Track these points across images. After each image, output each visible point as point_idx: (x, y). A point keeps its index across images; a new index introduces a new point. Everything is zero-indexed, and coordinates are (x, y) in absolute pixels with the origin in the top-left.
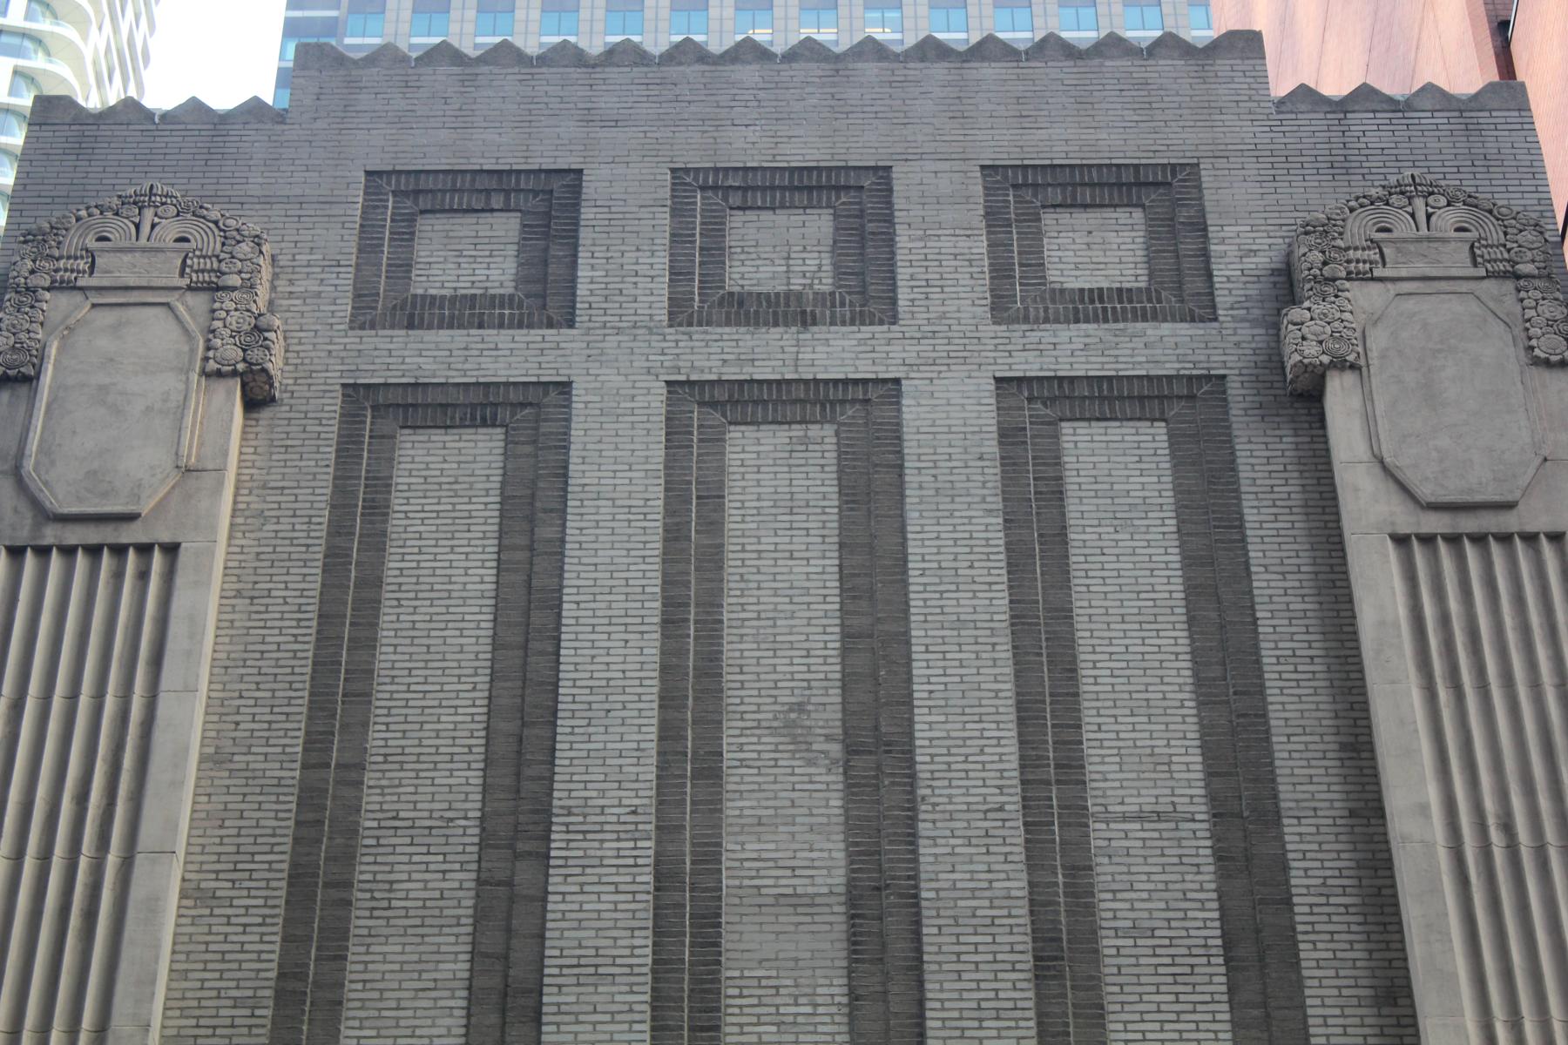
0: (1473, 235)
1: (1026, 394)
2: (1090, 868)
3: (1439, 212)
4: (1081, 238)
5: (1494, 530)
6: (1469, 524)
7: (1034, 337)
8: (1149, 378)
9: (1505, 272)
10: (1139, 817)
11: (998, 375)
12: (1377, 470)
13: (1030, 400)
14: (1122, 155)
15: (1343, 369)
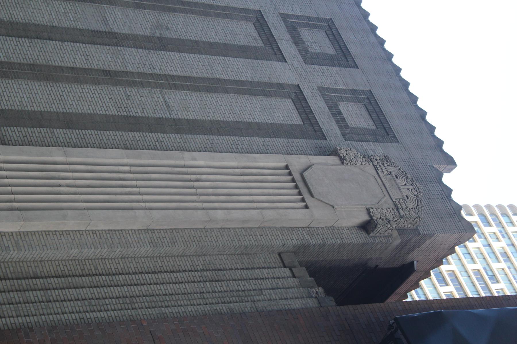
0: (407, 200)
1: (296, 91)
2: (143, 87)
3: (411, 192)
4: (358, 112)
5: (301, 191)
6: (304, 190)
7: (317, 95)
8: (317, 121)
9: (397, 206)
10: (165, 101)
11: (300, 85)
12: (309, 164)
13: (295, 92)
14: (393, 124)
15: (341, 160)
